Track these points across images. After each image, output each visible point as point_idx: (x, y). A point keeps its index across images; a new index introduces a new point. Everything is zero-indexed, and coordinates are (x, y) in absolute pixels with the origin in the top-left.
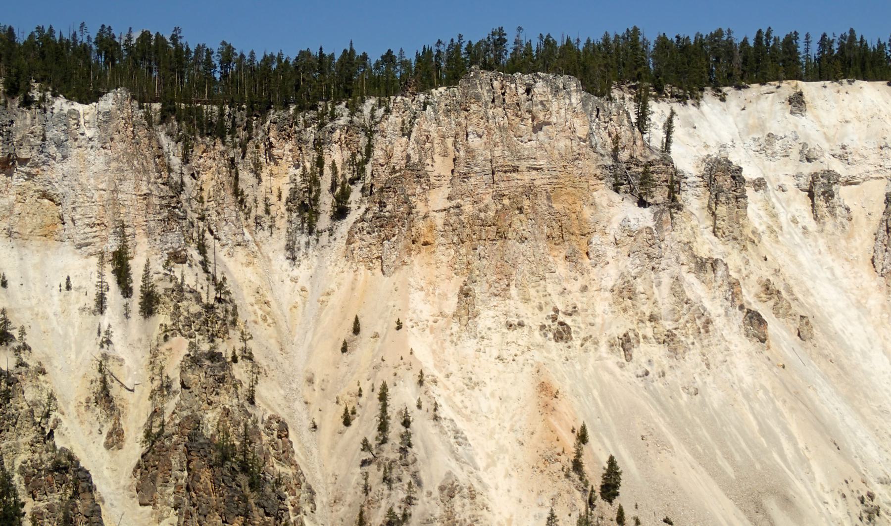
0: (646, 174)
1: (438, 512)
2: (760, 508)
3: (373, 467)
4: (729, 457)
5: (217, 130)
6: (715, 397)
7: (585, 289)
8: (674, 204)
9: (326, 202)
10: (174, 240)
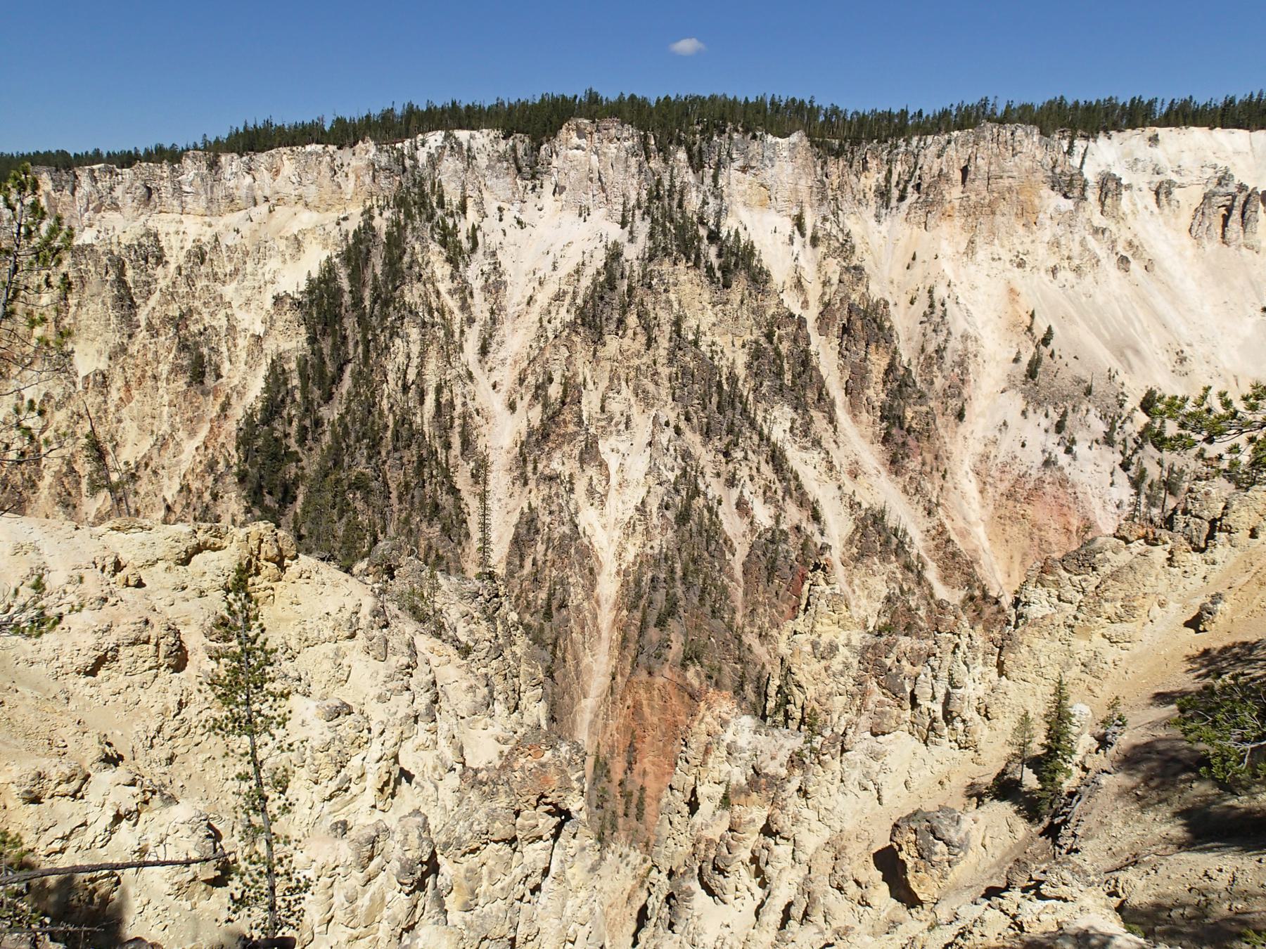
0: (1071, 180)
1: (960, 347)
2: (1122, 354)
3: (927, 325)
4: (1107, 328)
5: (838, 154)
6: (1100, 299)
7: (1033, 242)
8: (1083, 198)
9: (895, 193)
10: (825, 210)
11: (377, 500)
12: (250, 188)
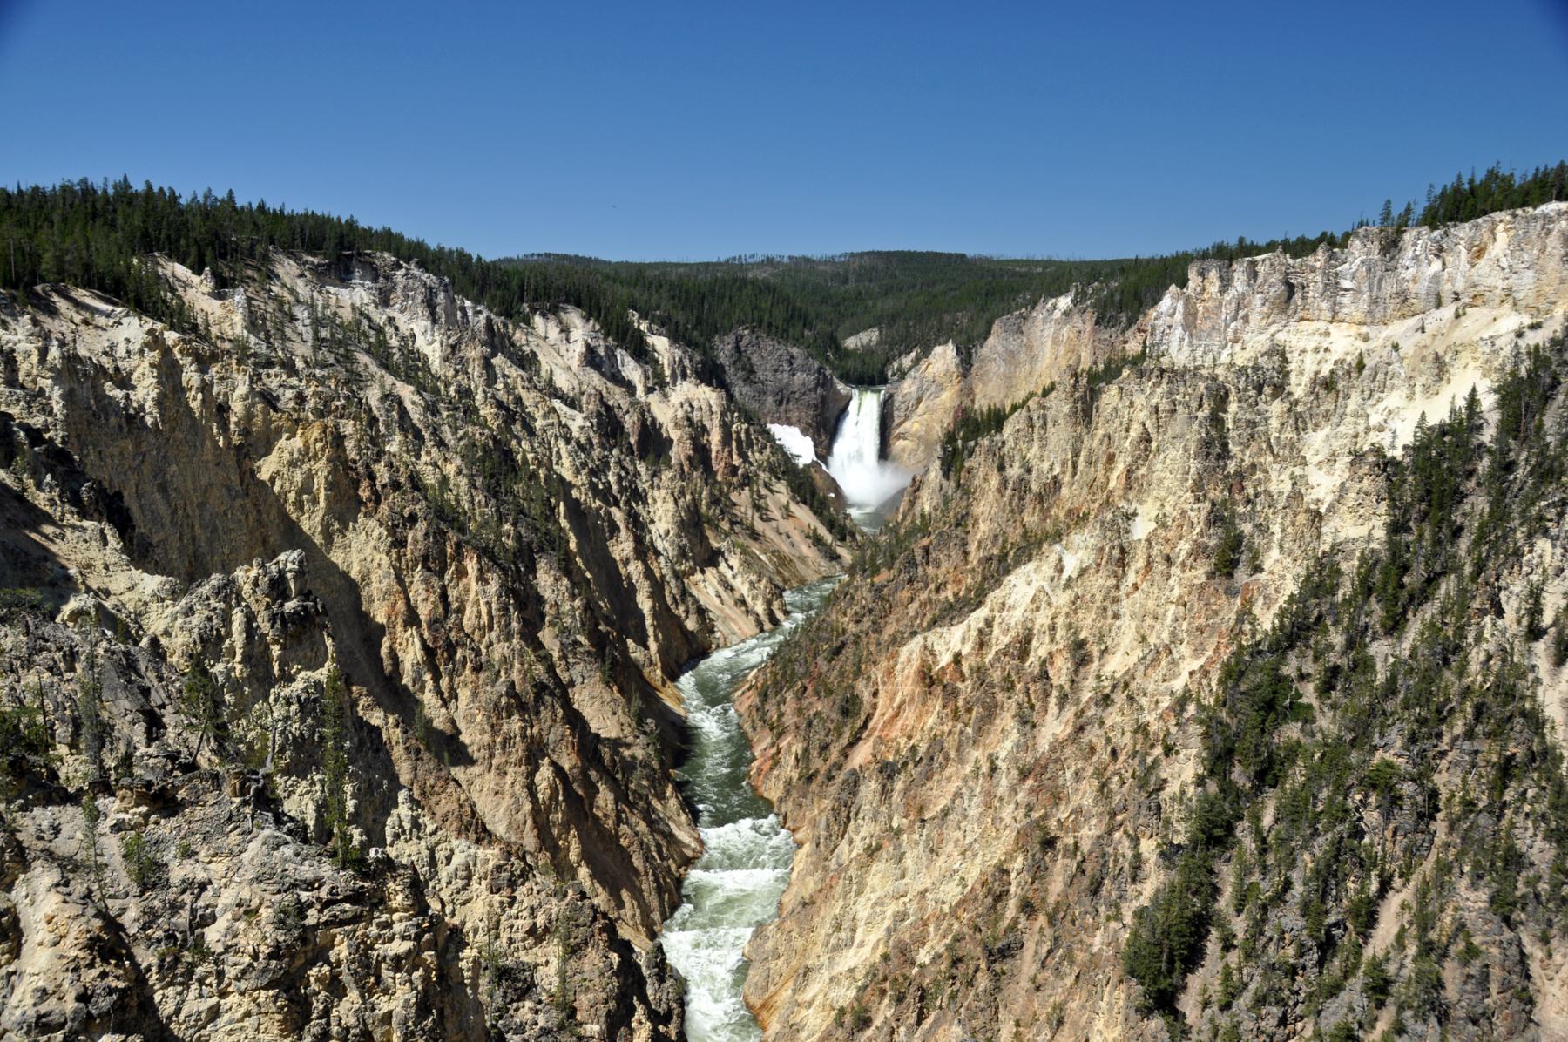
11: (1405, 818)
12: (1436, 279)
